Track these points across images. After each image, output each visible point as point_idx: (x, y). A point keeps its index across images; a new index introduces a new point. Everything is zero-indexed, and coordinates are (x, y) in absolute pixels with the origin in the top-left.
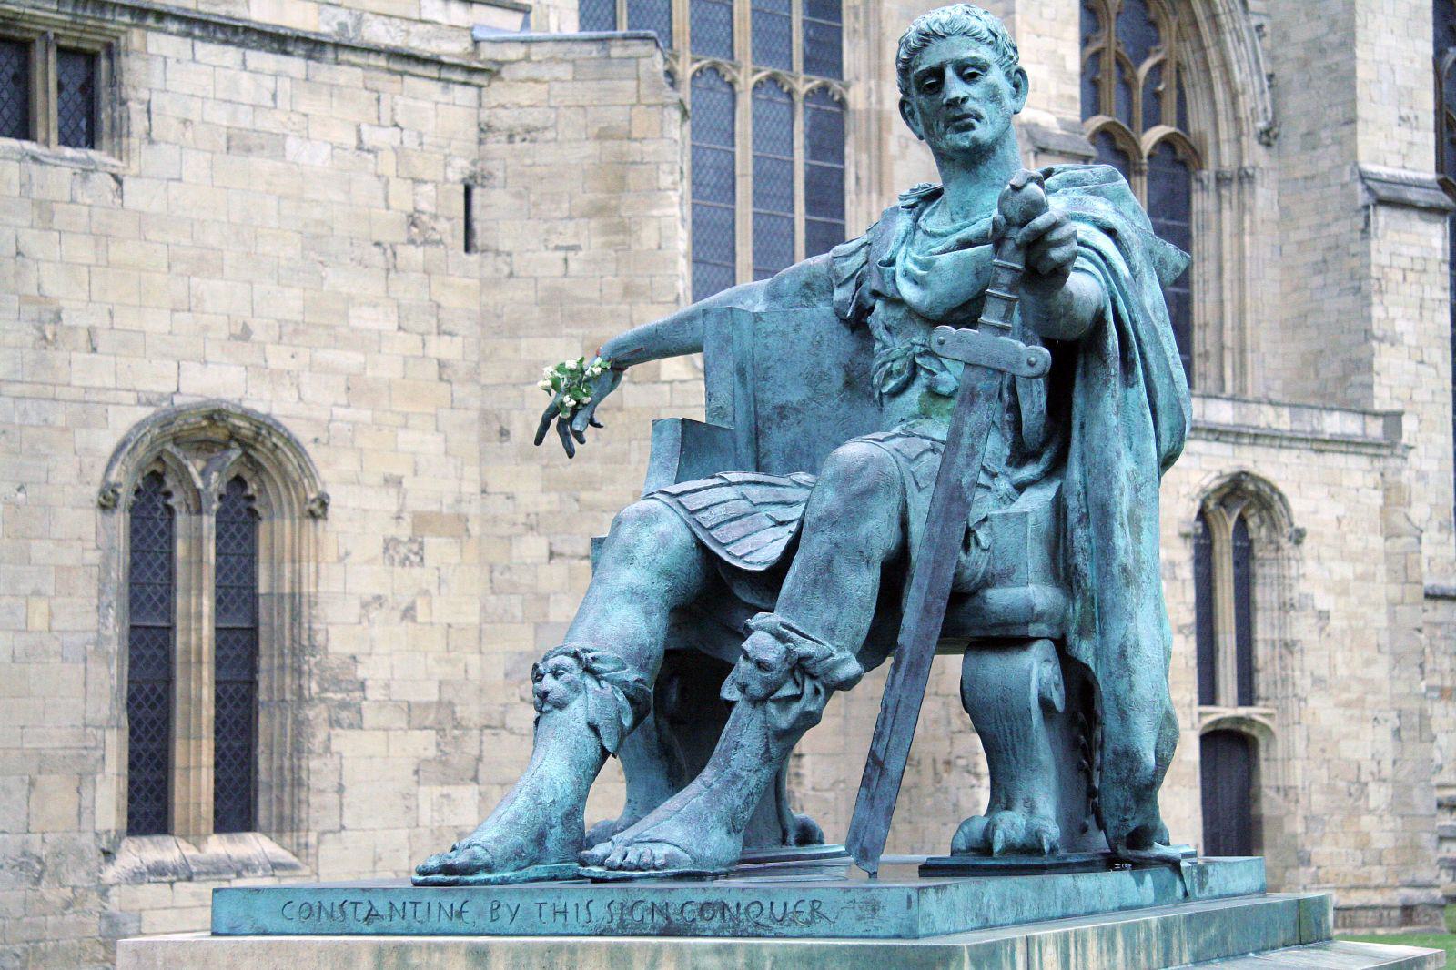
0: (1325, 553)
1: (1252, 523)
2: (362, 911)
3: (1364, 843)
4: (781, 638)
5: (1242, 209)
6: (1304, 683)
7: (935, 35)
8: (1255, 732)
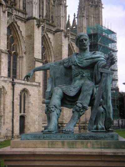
0: (33, 97)
1: (25, 94)
2: (42, 137)
3: (35, 128)
4: (81, 104)
5: (22, 60)
6: (30, 111)
7: (82, 36)
8: (25, 116)
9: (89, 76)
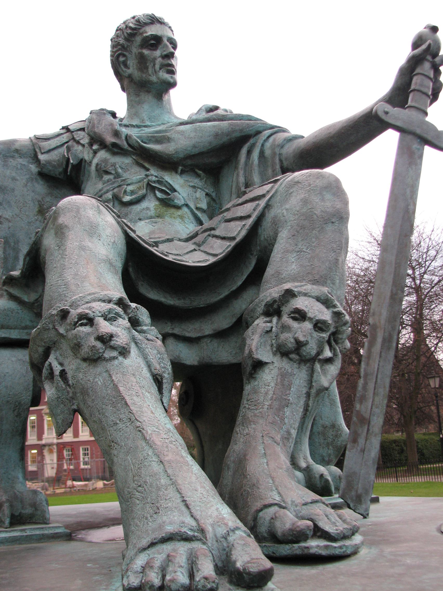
9: (204, 205)
